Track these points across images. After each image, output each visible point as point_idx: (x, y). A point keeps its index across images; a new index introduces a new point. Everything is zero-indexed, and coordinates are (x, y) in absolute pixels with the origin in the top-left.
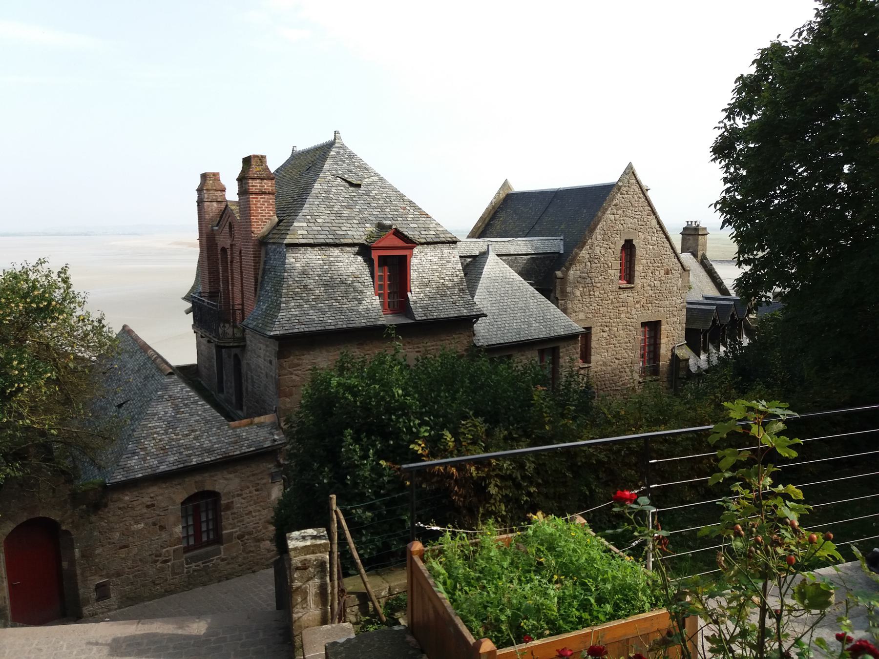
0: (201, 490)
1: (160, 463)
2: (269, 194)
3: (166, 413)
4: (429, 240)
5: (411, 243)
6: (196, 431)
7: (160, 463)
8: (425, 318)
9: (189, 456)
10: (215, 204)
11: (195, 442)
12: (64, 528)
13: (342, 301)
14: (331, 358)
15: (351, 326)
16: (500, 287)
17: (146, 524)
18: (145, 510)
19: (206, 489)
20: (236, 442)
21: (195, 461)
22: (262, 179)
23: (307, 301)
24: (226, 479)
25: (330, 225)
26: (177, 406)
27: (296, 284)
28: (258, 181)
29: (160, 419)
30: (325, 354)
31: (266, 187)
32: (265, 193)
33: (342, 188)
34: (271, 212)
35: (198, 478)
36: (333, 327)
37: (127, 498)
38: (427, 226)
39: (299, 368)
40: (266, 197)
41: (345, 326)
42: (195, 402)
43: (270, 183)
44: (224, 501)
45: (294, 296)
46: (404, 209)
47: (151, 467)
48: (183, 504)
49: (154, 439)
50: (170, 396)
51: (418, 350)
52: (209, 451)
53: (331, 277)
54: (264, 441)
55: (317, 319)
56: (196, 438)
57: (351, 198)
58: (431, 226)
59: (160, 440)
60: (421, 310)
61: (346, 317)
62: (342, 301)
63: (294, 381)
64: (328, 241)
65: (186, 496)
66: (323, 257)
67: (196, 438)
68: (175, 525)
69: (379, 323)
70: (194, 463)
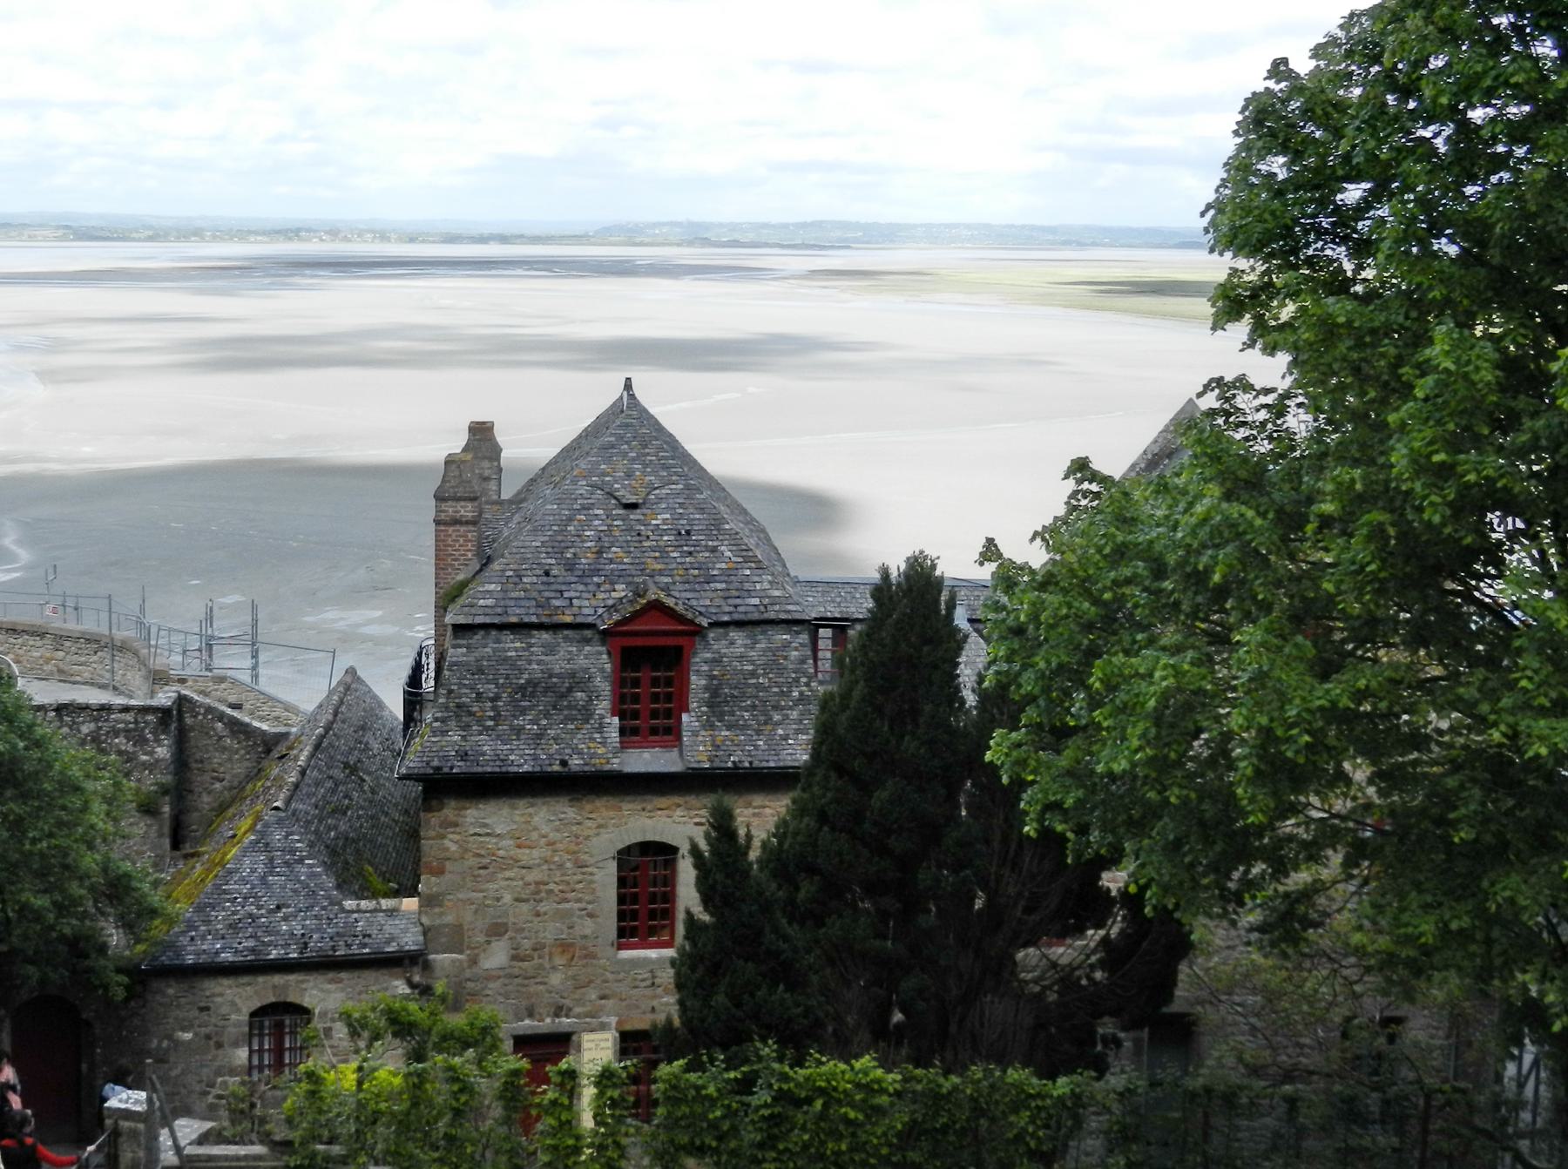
0: (282, 999)
2: (467, 523)
3: (253, 871)
4: (736, 617)
9: (269, 944)
12: (84, 1016)
14: (517, 819)
17: (196, 1034)
18: (196, 1013)
19: (289, 1000)
21: (274, 954)
22: (459, 499)
23: (480, 721)
24: (322, 990)
28: (450, 503)
30: (505, 811)
31: (462, 513)
34: (470, 554)
35: (278, 979)
36: (515, 769)
37: (171, 991)
38: (747, 586)
39: (458, 830)
40: (463, 529)
43: (470, 506)
44: (317, 1024)
46: (714, 550)
48: (253, 1015)
51: (697, 820)
54: (388, 942)
56: (285, 919)
58: (758, 586)
59: (234, 913)
64: (526, 620)
65: (259, 1005)
66: (518, 645)
70: (272, 957)
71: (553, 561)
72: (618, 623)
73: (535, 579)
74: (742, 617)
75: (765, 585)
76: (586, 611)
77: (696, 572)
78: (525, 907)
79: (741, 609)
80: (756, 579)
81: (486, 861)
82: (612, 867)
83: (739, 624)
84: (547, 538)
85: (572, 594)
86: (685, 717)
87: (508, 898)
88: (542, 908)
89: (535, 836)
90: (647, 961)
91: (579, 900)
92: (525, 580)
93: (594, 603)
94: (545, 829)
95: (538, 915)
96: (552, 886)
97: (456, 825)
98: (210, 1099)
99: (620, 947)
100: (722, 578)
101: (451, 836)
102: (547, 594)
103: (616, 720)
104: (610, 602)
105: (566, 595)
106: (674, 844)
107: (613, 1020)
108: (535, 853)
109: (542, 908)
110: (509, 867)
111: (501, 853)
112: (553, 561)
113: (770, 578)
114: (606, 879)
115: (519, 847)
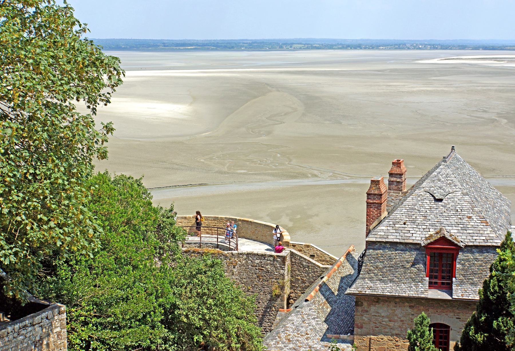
4: (475, 244)
5: (458, 249)
6: (309, 334)
8: (461, 297)
11: (306, 340)
13: (401, 278)
15: (401, 295)
23: (376, 275)
25: (402, 229)
27: (371, 265)
29: (293, 323)
36: (389, 294)
39: (368, 313)
41: (397, 294)
45: (369, 271)
55: (380, 287)
58: (486, 232)
60: (460, 291)
61: (400, 288)
62: (401, 278)
63: (364, 320)
67: (307, 339)
71: (408, 219)
72: (429, 244)
73: (400, 226)
74: (478, 244)
75: (488, 232)
76: (417, 238)
77: (462, 226)
80: (485, 229)
81: (377, 326)
83: (476, 247)
84: (406, 211)
85: (413, 232)
86: (454, 279)
92: (396, 226)
93: (422, 236)
100: (472, 229)
101: (365, 315)
102: (404, 231)
103: (428, 278)
104: (427, 236)
105: (411, 232)
108: (396, 324)
111: (384, 323)
112: (408, 219)
113: (491, 229)
115: (390, 321)
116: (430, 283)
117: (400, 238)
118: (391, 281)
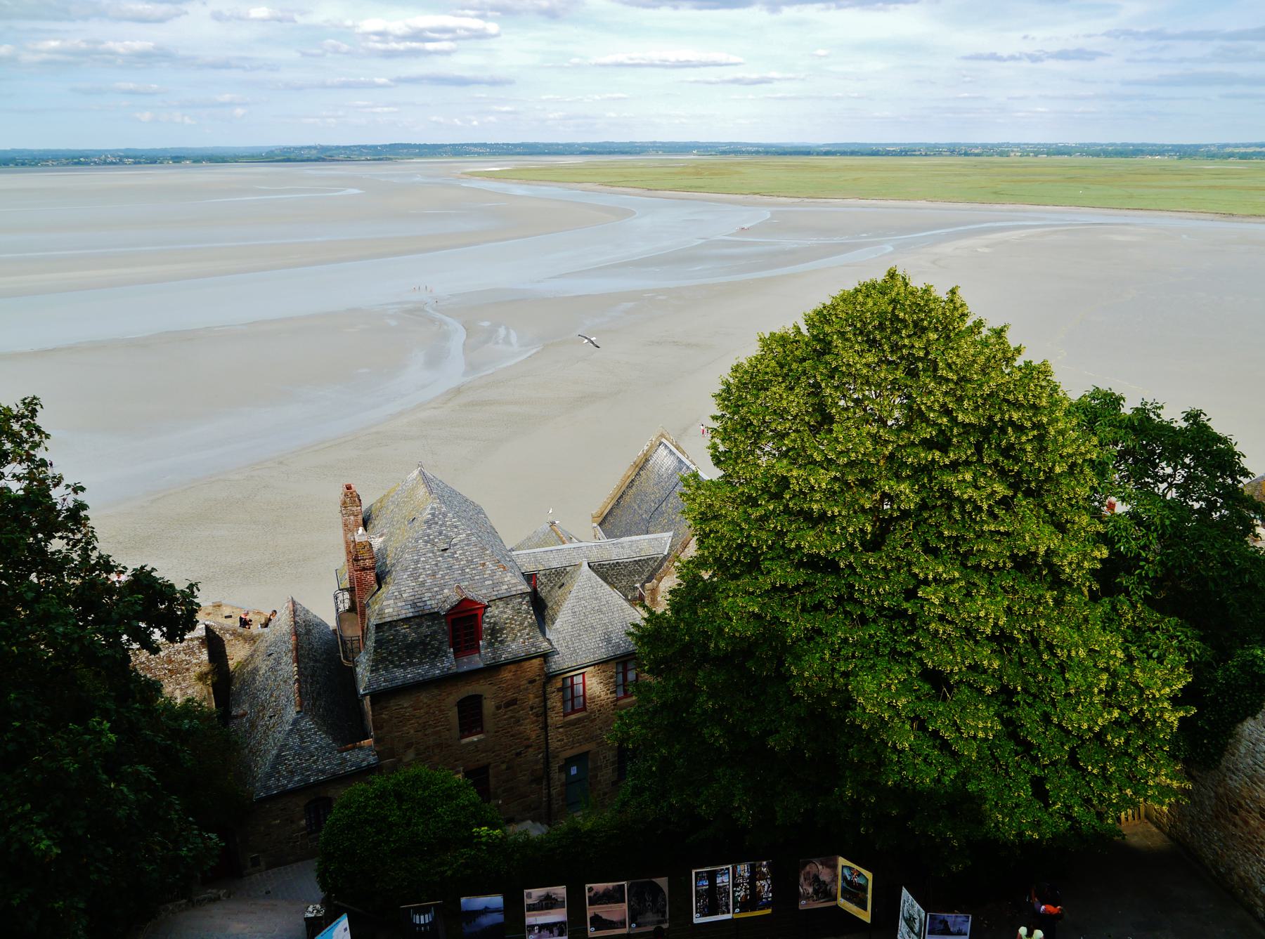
1: (289, 782)
7: (289, 782)
9: (309, 776)
10: (352, 518)
16: (586, 604)
20: (340, 764)
23: (392, 662)
26: (302, 737)
32: (367, 569)
33: (431, 555)
37: (268, 806)
41: (421, 679)
42: (315, 733)
46: (484, 564)
47: (283, 785)
49: (285, 764)
50: (297, 730)
52: (323, 772)
53: (412, 641)
56: (314, 762)
57: (436, 565)
59: (290, 765)
68: (301, 819)
69: (451, 672)
75: (509, 578)
78: (419, 733)
79: (500, 592)
82: (456, 709)
86: (481, 643)
87: (412, 731)
88: (427, 732)
89: (421, 704)
90: (474, 742)
91: (442, 725)
94: (425, 700)
95: (426, 735)
96: (431, 722)
97: (386, 707)
98: (291, 844)
99: (462, 737)
103: (452, 650)
106: (479, 693)
107: (461, 769)
108: (422, 711)
109: (427, 732)
110: (412, 719)
114: (453, 714)
116: (455, 653)
117: (412, 610)
118: (411, 664)
